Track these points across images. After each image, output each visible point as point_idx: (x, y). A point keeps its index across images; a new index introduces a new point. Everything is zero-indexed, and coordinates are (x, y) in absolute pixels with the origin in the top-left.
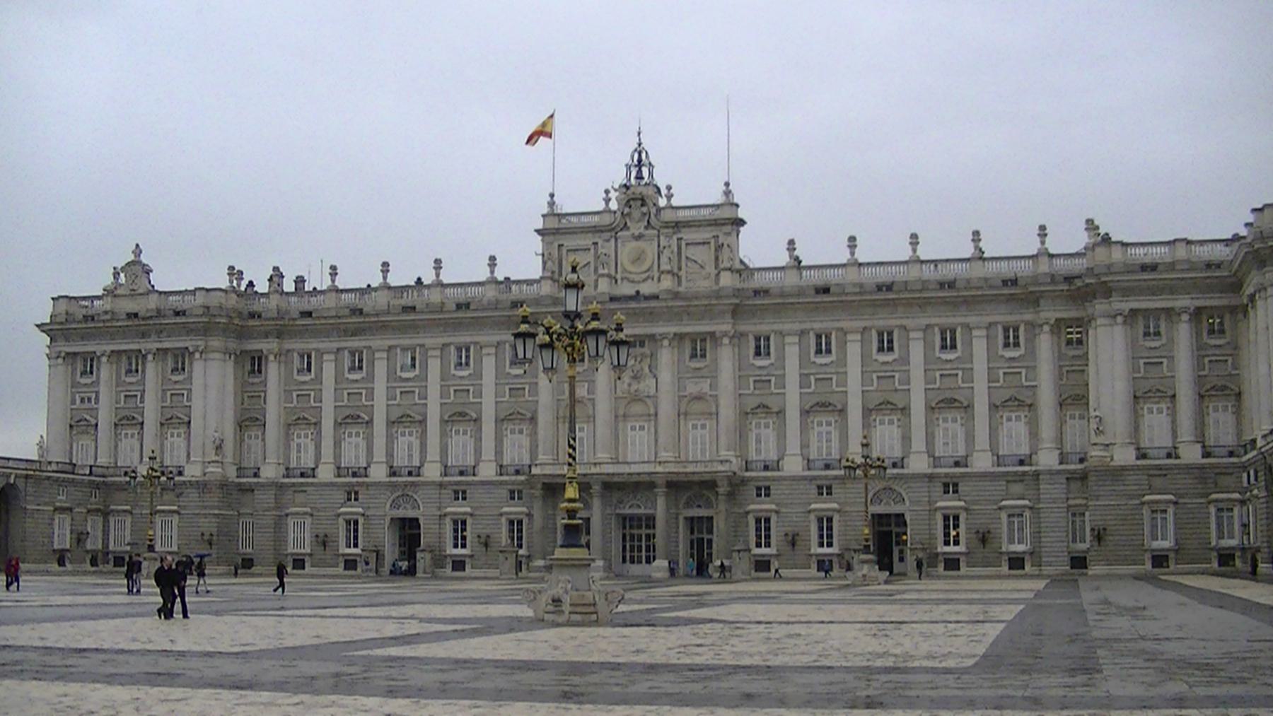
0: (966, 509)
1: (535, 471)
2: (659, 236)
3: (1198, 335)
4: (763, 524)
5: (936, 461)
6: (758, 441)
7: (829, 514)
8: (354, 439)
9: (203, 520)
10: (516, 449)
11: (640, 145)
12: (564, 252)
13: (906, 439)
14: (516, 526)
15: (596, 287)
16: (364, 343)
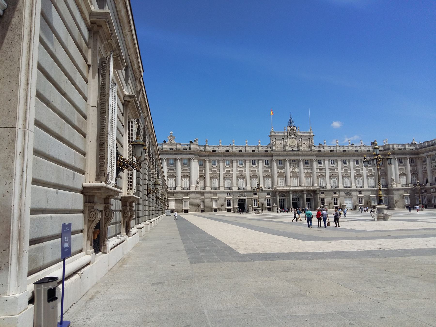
2: (297, 138)
3: (410, 163)
6: (321, 181)
9: (197, 201)
11: (291, 117)
12: (276, 140)
13: (351, 182)
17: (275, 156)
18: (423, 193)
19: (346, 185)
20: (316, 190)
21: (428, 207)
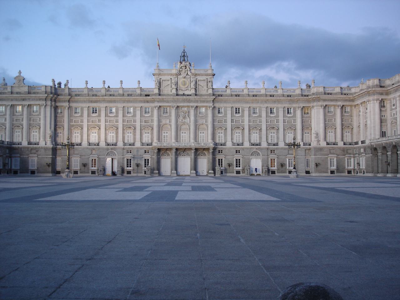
0: (277, 157)
1: (154, 144)
4: (220, 161)
5: (269, 144)
6: (219, 137)
7: (239, 158)
8: (94, 134)
10: (147, 138)
11: (184, 50)
14: (147, 162)
15: (171, 91)
16: (98, 105)
17: (158, 102)
18: (356, 154)
19: (254, 141)
20: (209, 148)
21: (358, 172)
